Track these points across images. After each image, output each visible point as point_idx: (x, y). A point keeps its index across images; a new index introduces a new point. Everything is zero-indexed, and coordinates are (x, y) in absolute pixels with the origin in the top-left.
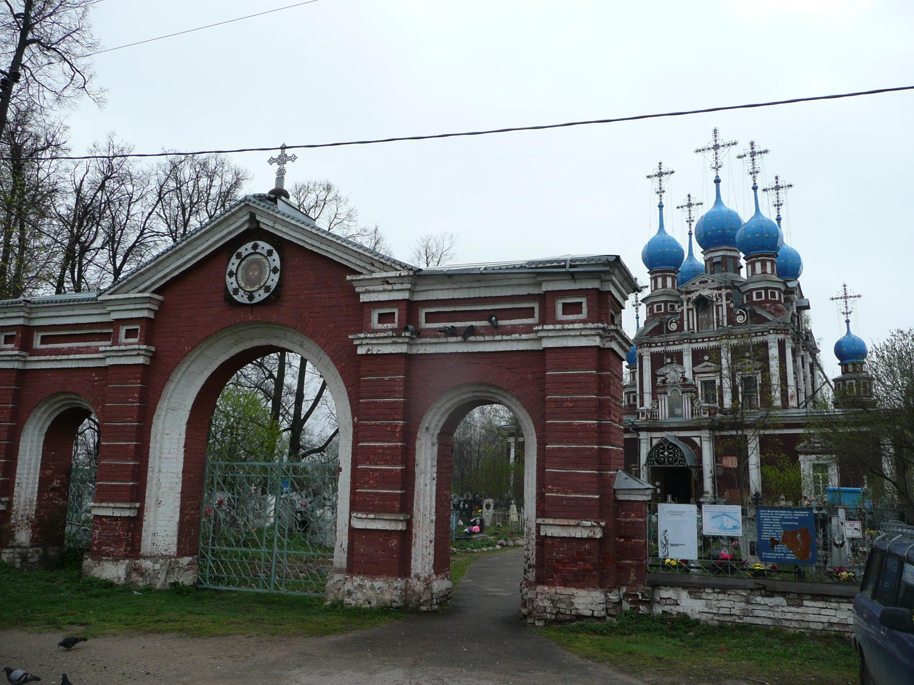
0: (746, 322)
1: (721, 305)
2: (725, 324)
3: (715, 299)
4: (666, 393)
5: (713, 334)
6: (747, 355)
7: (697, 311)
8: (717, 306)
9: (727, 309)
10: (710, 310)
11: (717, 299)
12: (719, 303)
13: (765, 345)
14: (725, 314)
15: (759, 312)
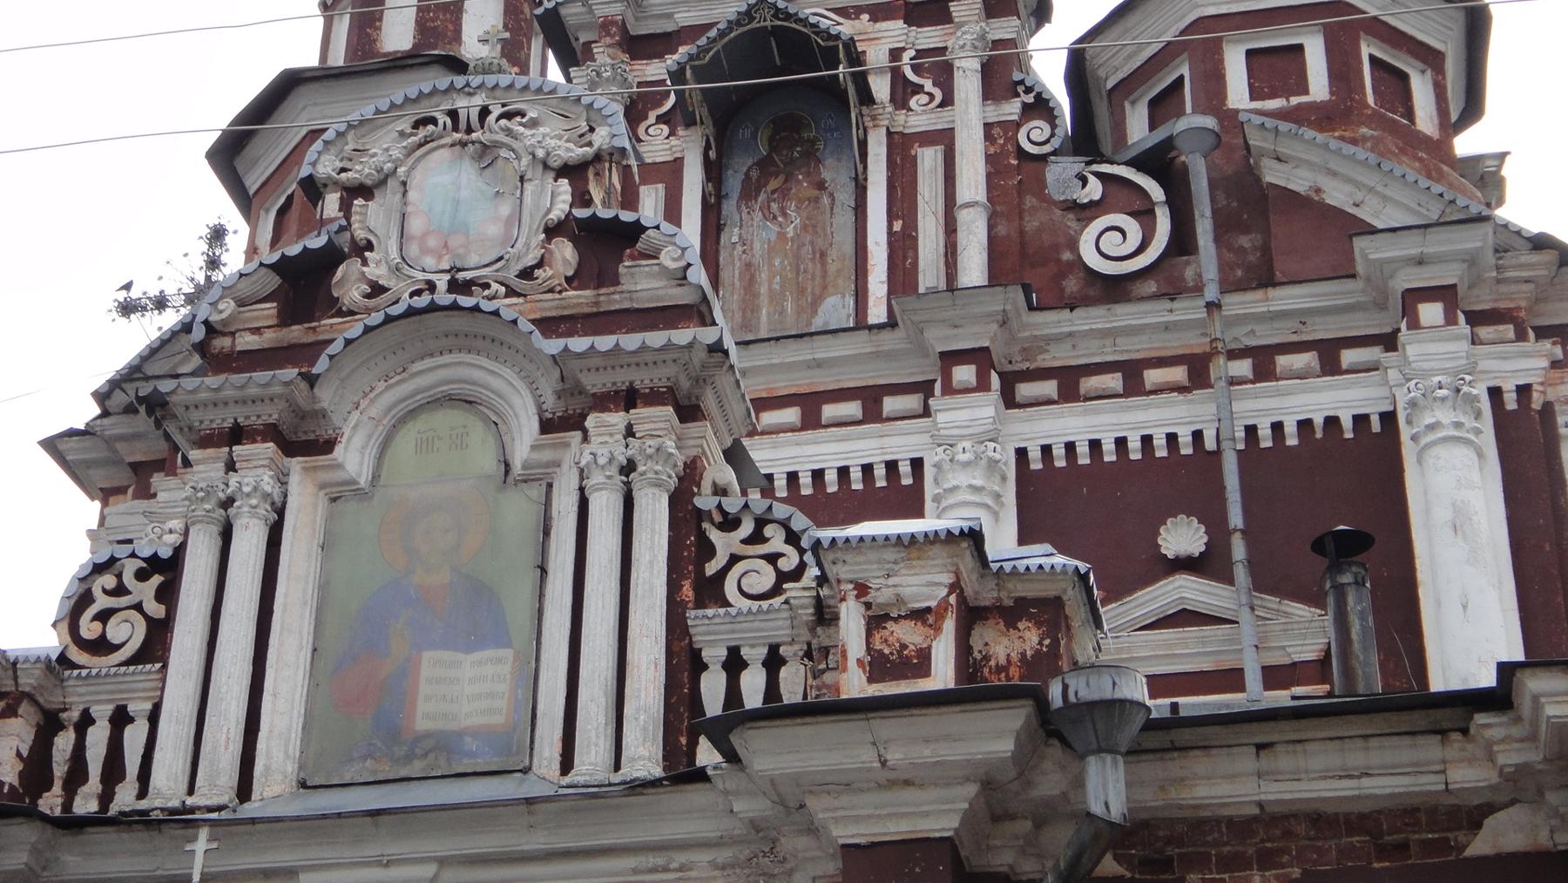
0: (1167, 277)
1: (945, 139)
2: (973, 270)
3: (881, 88)
4: (304, 440)
5: (850, 360)
6: (1182, 537)
7: (714, 172)
8: (901, 148)
9: (993, 162)
10: (835, 173)
11: (903, 91)
12: (920, 117)
13: (1367, 463)
14: (972, 181)
15: (1301, 167)
